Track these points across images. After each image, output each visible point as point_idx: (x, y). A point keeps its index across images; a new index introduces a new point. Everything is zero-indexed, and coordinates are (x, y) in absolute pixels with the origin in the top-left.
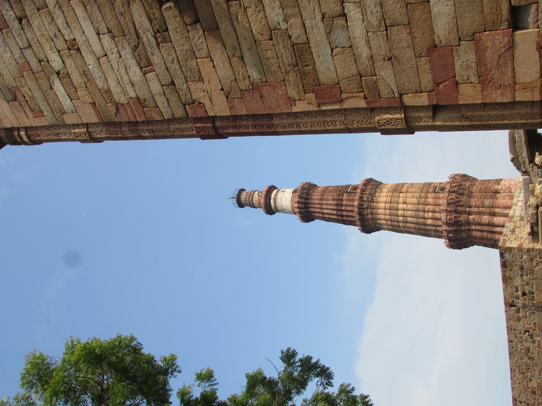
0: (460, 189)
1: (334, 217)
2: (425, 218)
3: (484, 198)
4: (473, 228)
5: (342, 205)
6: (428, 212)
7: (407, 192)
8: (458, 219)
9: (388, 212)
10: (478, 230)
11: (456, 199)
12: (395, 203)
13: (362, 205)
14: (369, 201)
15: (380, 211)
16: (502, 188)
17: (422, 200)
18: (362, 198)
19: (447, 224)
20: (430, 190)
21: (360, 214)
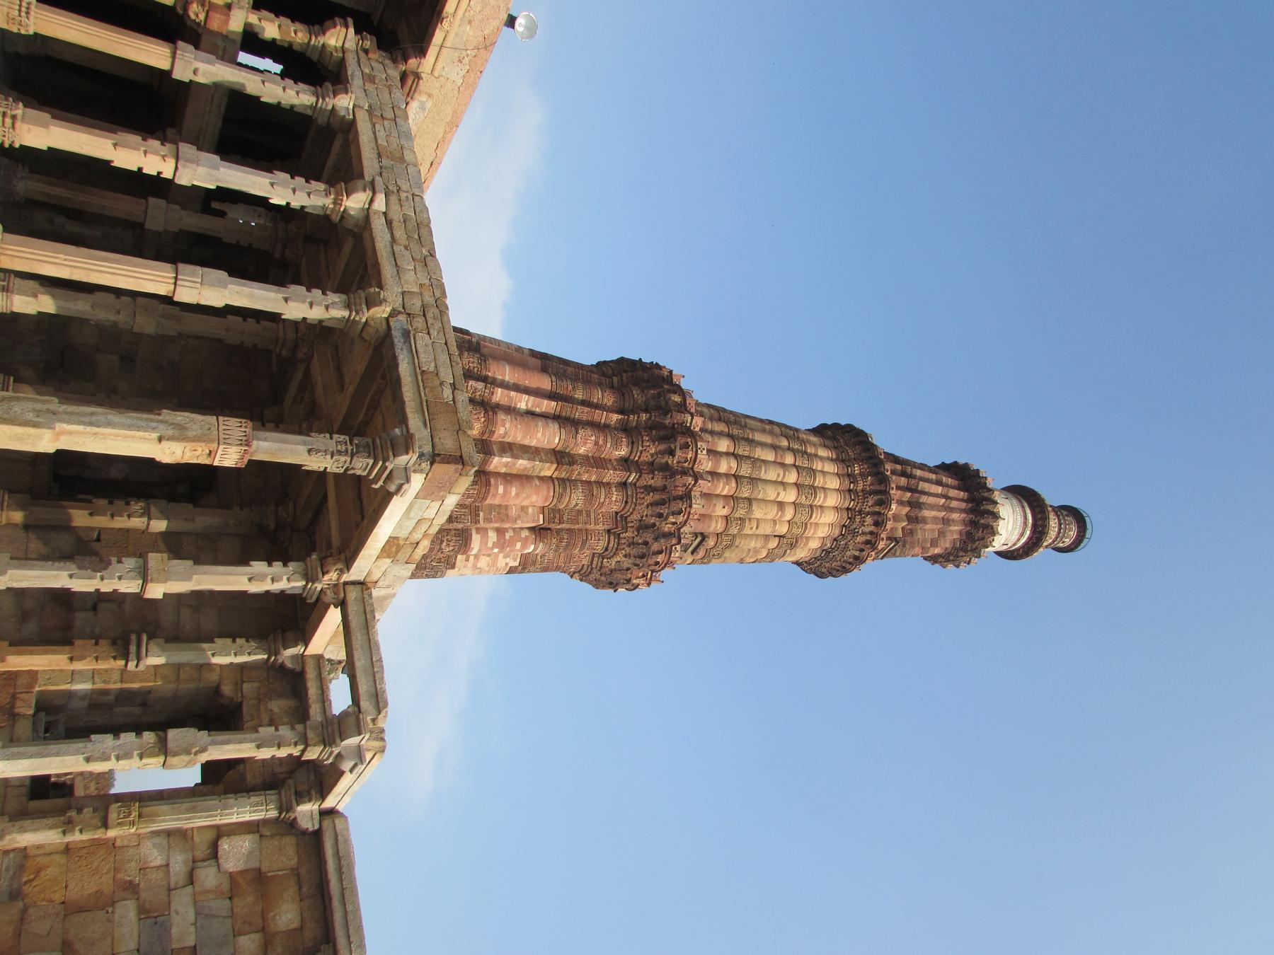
0: (646, 543)
1: (918, 473)
2: (735, 456)
3: (580, 512)
4: (615, 417)
5: (910, 503)
6: (727, 475)
7: (767, 537)
8: (662, 447)
9: (819, 481)
10: (597, 406)
11: (665, 511)
12: (803, 506)
13: (880, 503)
14: (860, 512)
15: (834, 483)
16: (524, 546)
17: (741, 512)
18: (876, 524)
19: (688, 432)
20: (711, 542)
21: (882, 479)
